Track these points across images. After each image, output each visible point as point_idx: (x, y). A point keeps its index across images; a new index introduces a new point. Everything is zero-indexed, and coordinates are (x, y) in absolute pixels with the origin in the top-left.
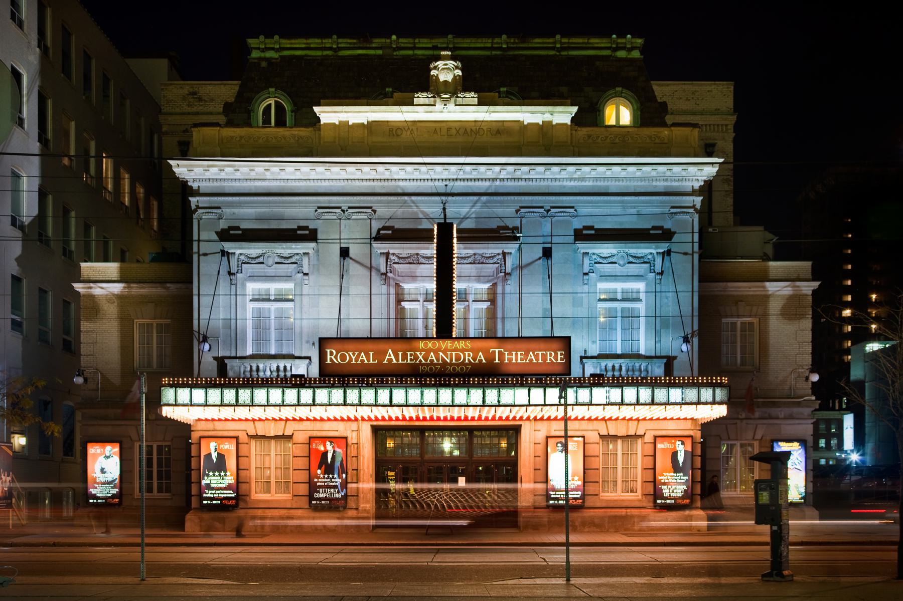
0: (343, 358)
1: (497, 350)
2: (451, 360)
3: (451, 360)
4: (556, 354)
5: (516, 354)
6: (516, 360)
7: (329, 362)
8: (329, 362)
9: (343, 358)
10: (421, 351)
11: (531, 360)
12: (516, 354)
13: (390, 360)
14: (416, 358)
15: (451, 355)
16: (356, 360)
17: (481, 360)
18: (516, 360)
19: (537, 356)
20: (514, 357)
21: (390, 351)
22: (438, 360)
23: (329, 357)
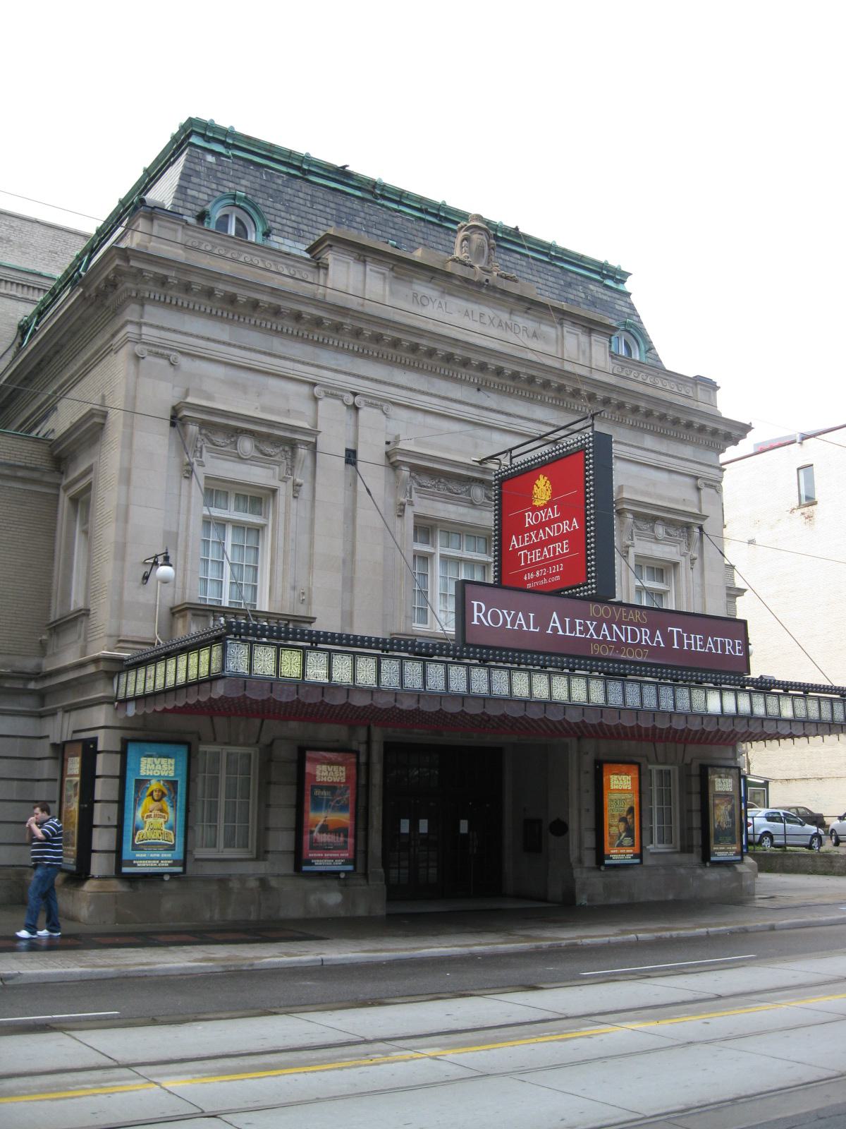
0: (495, 618)
1: (675, 630)
2: (627, 639)
3: (627, 639)
4: (734, 643)
5: (695, 638)
6: (696, 647)
7: (475, 622)
8: (475, 622)
9: (495, 618)
10: (592, 619)
11: (710, 648)
12: (695, 638)
13: (555, 629)
14: (586, 630)
15: (626, 629)
16: (513, 623)
17: (658, 642)
18: (696, 647)
19: (715, 643)
20: (693, 642)
21: (555, 615)
22: (612, 637)
23: (476, 614)
